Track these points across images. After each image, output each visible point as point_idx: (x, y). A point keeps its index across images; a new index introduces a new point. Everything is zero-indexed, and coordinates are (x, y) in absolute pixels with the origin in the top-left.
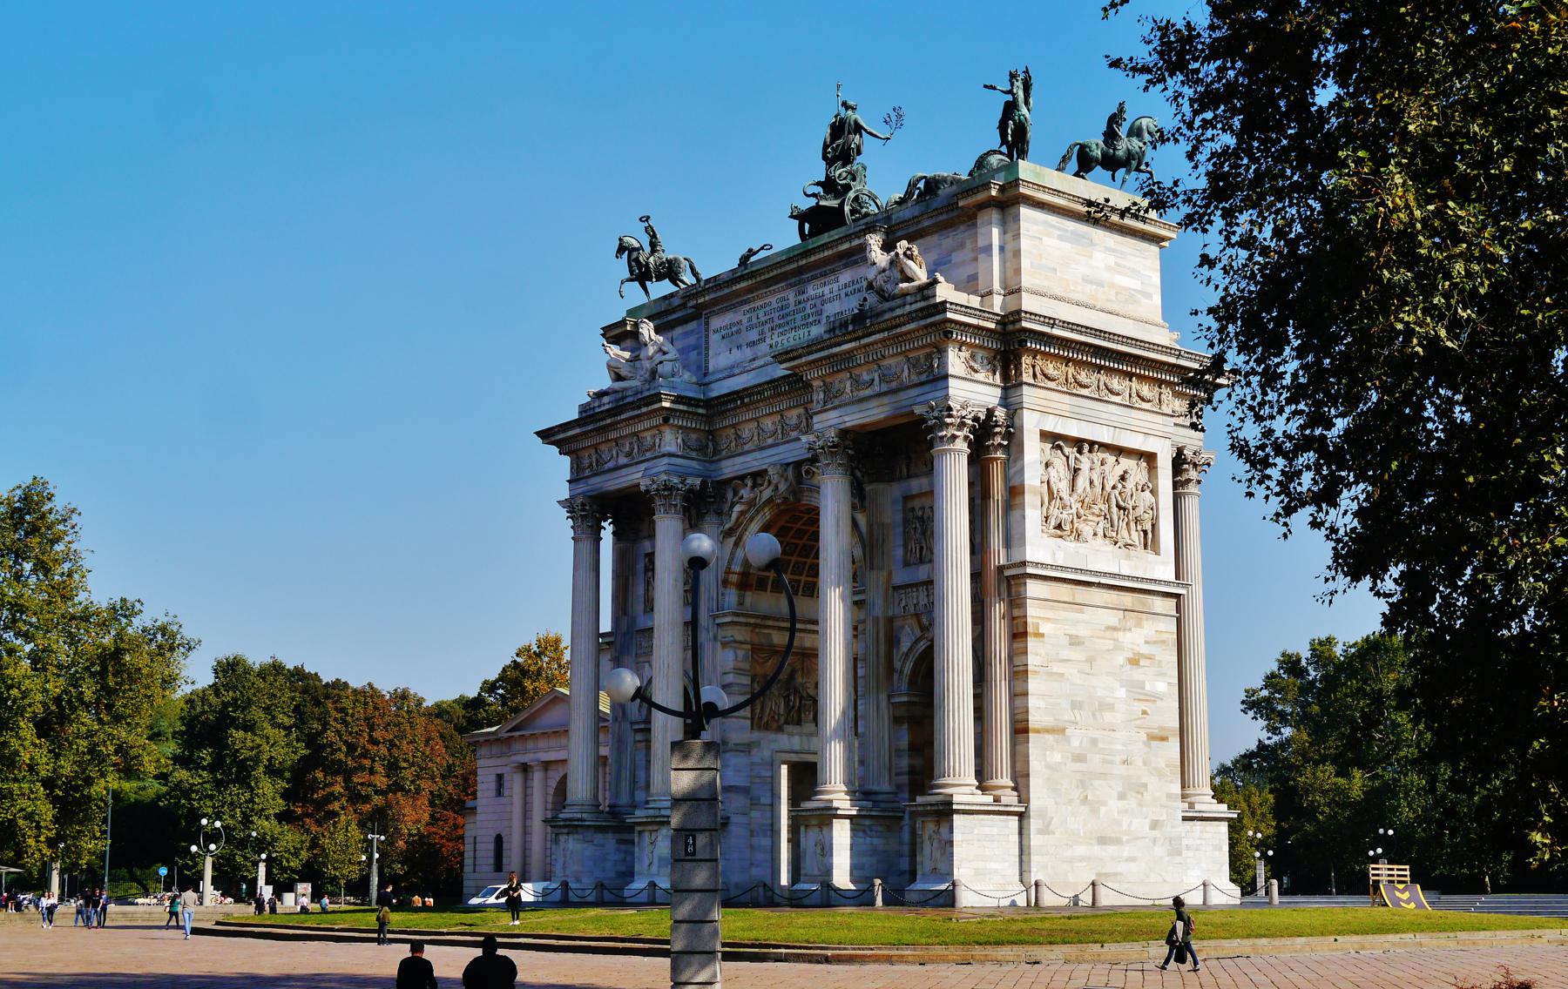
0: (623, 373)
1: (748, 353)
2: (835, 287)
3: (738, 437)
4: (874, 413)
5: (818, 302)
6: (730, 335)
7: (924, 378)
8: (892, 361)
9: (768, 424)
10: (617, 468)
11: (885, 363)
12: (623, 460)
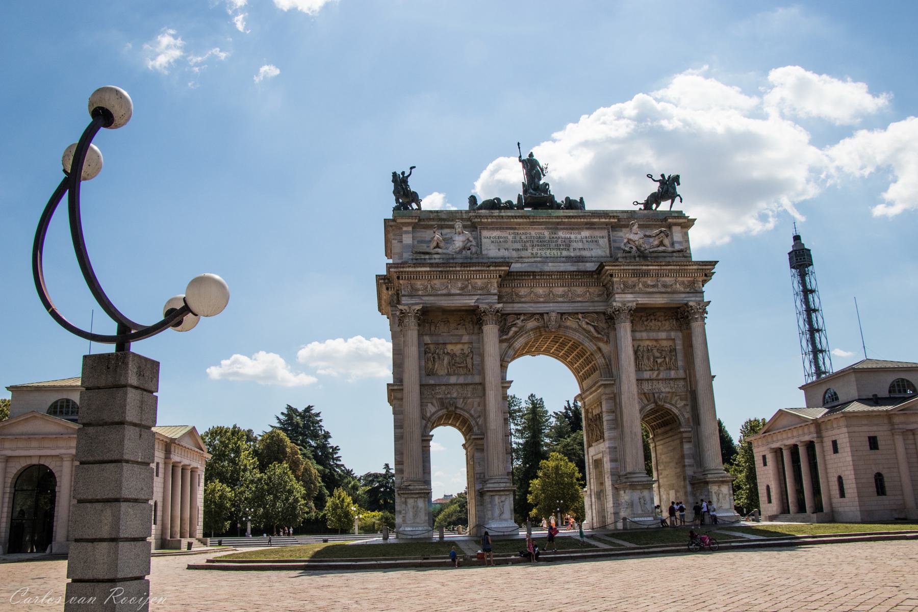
0: (442, 245)
1: (515, 254)
2: (579, 236)
3: (517, 295)
4: (659, 300)
5: (567, 241)
6: (497, 242)
7: (688, 290)
8: (667, 279)
9: (540, 291)
10: (450, 295)
11: (663, 279)
12: (453, 291)
